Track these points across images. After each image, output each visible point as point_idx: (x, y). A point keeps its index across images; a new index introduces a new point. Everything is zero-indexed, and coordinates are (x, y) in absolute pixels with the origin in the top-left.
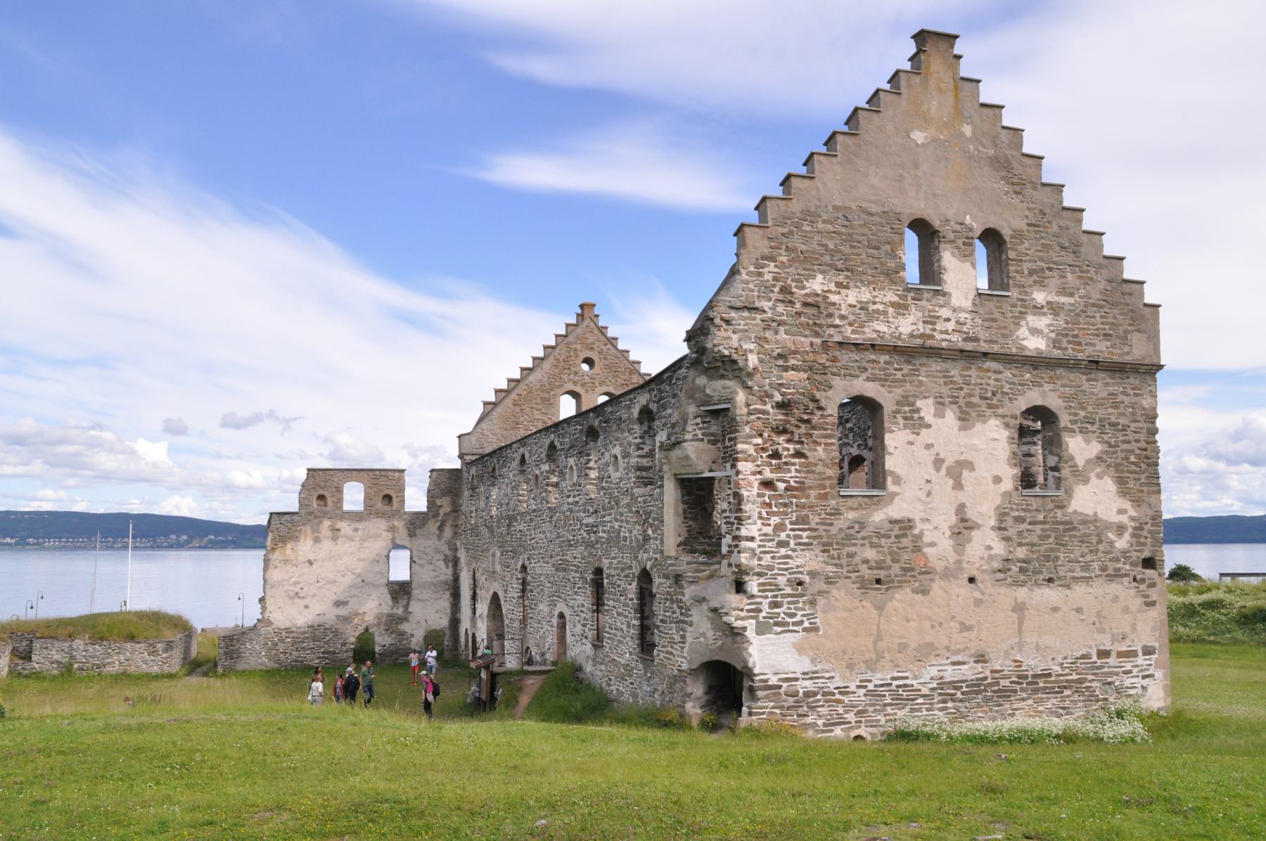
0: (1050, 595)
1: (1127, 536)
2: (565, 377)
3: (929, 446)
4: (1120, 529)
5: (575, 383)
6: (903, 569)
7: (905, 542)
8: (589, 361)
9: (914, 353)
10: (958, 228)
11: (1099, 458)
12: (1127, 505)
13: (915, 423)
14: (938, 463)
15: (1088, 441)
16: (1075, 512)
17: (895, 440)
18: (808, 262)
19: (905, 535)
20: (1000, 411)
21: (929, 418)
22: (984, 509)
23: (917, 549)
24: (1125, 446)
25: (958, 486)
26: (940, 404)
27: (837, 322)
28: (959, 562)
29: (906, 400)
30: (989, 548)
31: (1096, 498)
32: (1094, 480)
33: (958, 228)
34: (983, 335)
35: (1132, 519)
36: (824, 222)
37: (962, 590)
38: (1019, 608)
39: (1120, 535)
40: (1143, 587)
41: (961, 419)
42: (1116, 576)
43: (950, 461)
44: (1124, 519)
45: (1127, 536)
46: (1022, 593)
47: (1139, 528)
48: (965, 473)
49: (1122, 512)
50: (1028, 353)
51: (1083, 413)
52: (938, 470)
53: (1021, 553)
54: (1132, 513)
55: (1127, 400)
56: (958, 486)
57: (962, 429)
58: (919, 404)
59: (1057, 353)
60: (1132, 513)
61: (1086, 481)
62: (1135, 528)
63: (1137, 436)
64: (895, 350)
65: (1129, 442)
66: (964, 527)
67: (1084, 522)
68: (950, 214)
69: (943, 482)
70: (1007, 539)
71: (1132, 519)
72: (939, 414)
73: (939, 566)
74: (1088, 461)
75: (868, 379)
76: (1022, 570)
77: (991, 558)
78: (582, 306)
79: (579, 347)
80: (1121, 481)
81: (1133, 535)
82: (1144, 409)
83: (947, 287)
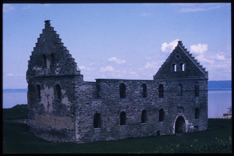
0: (58, 118)
1: (69, 108)
2: (173, 61)
3: (45, 92)
4: (69, 107)
5: (175, 62)
6: (43, 112)
7: (43, 107)
8: (178, 56)
9: (44, 77)
10: (48, 55)
11: (66, 93)
12: (69, 102)
13: (43, 88)
14: (46, 95)
15: (64, 90)
16: (62, 103)
17: (41, 91)
18: (34, 65)
19: (42, 106)
20: (53, 86)
21: (45, 88)
22: (51, 103)
23: (44, 109)
24: (69, 91)
25: (48, 99)
26: (46, 86)
27: (36, 73)
28: (48, 111)
29: (43, 85)
30: (51, 109)
31: (65, 101)
32: (65, 98)
33: (48, 55)
34: (51, 73)
35: (70, 105)
36: (35, 58)
37: (48, 115)
38: (55, 119)
39: (69, 108)
40: (72, 118)
41: (49, 88)
42: (68, 116)
43: (47, 95)
44: (69, 105)
45: (69, 108)
46: (55, 117)
47: (71, 107)
48: (49, 97)
49: (69, 104)
50: (56, 75)
51: (63, 85)
52: (46, 96)
53: (55, 110)
54: (70, 104)
55: (69, 82)
56: (48, 99)
57: (49, 89)
58: (44, 85)
59: (60, 75)
60: (70, 104)
61: (64, 98)
62: (71, 107)
63: (71, 89)
64: (41, 77)
65: (70, 90)
66: (49, 105)
67: (63, 105)
68: (47, 53)
69: (46, 98)
70: (54, 108)
71: (70, 105)
72: (46, 87)
73: (46, 111)
74: (64, 94)
75: (39, 82)
76: (56, 113)
77: (52, 111)
78: (178, 42)
79: (176, 53)
80: (69, 98)
81: (70, 108)
82: (72, 84)
83: (47, 66)
